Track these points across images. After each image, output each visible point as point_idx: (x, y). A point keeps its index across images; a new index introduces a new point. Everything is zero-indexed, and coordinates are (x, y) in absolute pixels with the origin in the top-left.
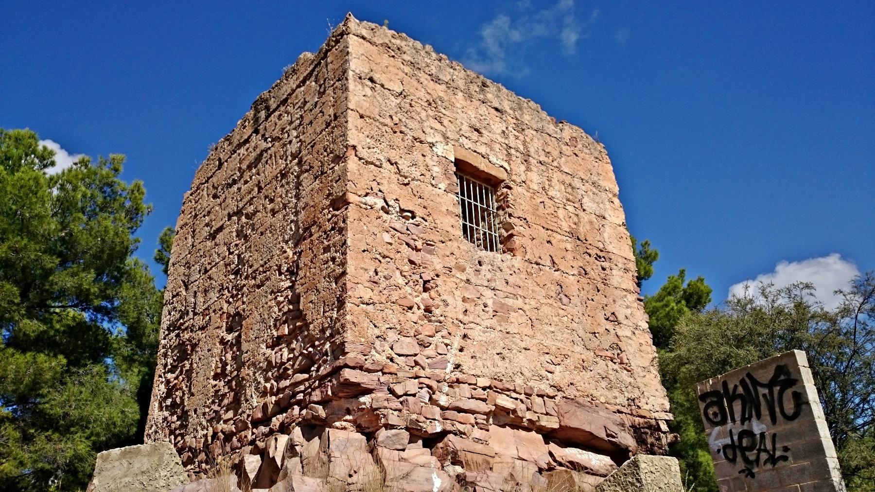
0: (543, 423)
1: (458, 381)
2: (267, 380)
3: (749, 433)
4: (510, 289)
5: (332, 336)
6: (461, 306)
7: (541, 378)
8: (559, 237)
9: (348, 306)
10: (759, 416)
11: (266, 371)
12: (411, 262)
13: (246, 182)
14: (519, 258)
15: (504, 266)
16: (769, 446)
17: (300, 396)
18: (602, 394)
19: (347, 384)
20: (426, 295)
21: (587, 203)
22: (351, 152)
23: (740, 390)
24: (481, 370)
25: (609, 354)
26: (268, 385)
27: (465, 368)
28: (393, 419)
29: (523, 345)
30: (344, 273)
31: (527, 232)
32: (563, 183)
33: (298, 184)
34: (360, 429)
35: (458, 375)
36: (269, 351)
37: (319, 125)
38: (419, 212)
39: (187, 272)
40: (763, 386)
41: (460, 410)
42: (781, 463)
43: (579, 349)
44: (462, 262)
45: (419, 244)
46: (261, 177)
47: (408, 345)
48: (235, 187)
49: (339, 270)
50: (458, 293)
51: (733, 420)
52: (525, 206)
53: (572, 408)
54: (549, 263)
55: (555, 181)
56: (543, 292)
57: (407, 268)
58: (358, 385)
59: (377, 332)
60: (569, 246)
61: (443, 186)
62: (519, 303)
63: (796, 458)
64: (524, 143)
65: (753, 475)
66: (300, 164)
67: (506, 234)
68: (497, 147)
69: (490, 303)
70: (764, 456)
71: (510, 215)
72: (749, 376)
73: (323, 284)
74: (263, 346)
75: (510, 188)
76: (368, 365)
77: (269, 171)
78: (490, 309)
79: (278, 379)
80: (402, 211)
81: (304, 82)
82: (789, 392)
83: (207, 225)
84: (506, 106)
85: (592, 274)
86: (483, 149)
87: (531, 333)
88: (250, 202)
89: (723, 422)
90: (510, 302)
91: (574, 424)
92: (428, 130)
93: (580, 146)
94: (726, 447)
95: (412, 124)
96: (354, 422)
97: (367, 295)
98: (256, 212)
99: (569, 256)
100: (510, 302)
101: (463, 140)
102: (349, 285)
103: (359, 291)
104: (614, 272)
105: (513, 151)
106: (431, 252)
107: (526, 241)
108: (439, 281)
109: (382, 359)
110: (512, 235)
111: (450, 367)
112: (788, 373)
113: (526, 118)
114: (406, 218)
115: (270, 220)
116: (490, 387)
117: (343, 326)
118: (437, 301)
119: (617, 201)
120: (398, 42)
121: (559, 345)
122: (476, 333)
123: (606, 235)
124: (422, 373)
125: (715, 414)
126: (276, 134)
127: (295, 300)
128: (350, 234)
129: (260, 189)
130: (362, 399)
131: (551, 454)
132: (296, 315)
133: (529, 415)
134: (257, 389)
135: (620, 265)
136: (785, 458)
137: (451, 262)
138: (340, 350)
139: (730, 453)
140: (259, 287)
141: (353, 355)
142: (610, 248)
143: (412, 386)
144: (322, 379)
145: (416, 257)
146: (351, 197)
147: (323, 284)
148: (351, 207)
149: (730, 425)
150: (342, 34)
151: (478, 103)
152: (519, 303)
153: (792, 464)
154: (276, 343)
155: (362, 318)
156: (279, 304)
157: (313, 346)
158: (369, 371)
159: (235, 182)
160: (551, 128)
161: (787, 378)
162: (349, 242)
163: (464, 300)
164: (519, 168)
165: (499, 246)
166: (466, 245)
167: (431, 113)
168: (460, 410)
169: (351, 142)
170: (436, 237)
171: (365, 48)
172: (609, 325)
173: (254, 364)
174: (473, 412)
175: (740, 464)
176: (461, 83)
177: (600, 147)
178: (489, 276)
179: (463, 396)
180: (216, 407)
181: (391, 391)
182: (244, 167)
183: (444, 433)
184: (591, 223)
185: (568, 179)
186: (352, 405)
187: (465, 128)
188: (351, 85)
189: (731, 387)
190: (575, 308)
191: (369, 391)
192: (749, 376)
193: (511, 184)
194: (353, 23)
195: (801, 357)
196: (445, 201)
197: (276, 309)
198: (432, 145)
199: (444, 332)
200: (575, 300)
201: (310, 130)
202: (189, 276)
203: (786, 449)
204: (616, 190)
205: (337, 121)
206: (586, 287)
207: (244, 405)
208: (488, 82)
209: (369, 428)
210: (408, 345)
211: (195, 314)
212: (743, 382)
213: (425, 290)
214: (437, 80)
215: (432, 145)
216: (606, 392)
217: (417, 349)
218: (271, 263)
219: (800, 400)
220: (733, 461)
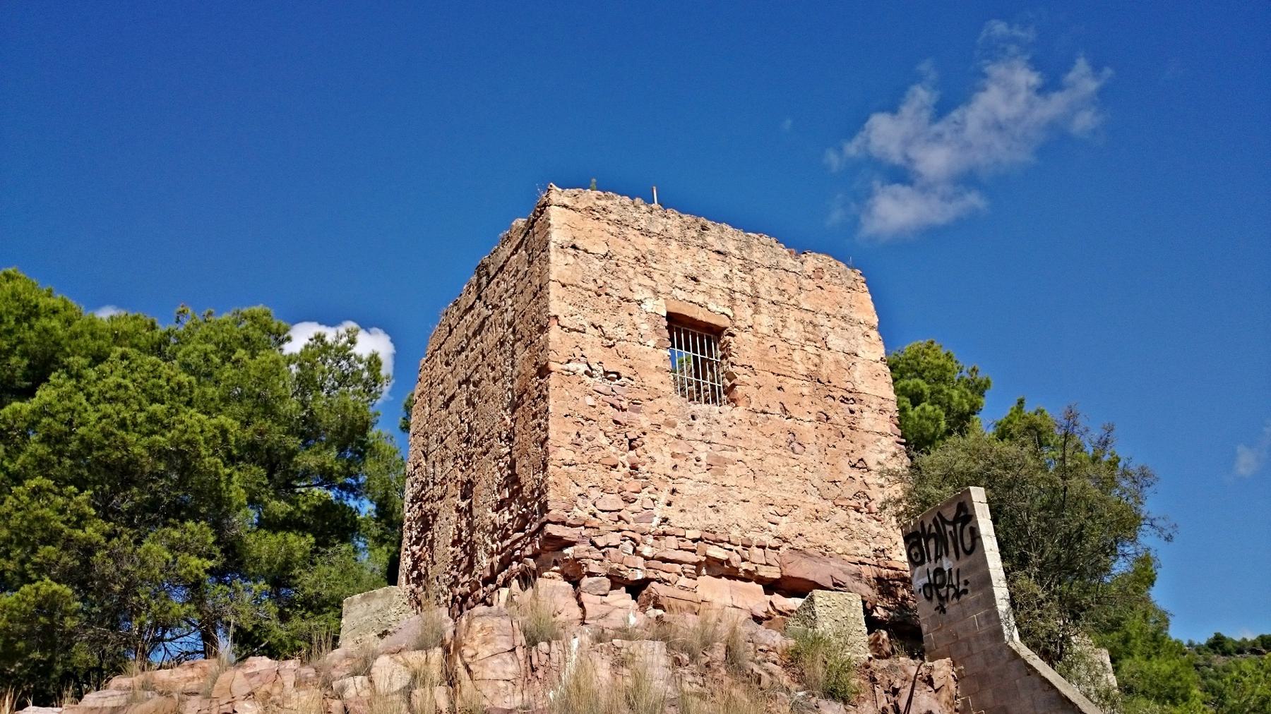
0: (761, 574)
1: (665, 534)
2: (494, 542)
3: (939, 571)
4: (728, 441)
5: (539, 496)
6: (670, 462)
7: (763, 529)
8: (794, 382)
9: (551, 468)
10: (947, 555)
11: (492, 533)
12: (616, 422)
13: (472, 350)
14: (741, 408)
15: (722, 418)
16: (955, 582)
17: (517, 553)
18: (839, 544)
19: (550, 538)
20: (632, 453)
21: (833, 341)
22: (553, 323)
23: (934, 529)
24: (691, 522)
25: (854, 503)
26: (495, 546)
27: (672, 521)
28: (594, 567)
29: (742, 497)
30: (547, 438)
31: (752, 380)
32: (802, 322)
33: (513, 353)
34: (567, 578)
35: (666, 528)
36: (494, 515)
37: (528, 296)
38: (625, 372)
39: (425, 442)
40: (949, 523)
41: (665, 560)
42: (963, 597)
43: (813, 498)
44: (672, 418)
45: (625, 404)
46: (484, 345)
47: (613, 501)
48: (464, 354)
49: (543, 436)
50: (666, 449)
51: (930, 560)
52: (751, 352)
53: (797, 558)
54: (778, 411)
55: (791, 321)
56: (770, 442)
57: (611, 428)
58: (560, 538)
59: (579, 490)
60: (805, 391)
61: (652, 343)
62: (740, 454)
63: (973, 591)
64: (753, 284)
65: (944, 611)
66: (514, 333)
67: (729, 384)
68: (717, 293)
69: (703, 457)
70: (952, 591)
71: (732, 364)
72: (939, 514)
73: (532, 449)
74: (490, 510)
75: (733, 335)
76: (570, 520)
77: (491, 338)
78: (703, 463)
79: (502, 540)
80: (606, 373)
81: (516, 250)
82: (967, 527)
83: (441, 393)
84: (731, 247)
85: (835, 418)
86: (700, 298)
87: (752, 484)
88: (476, 370)
89: (922, 562)
90: (727, 454)
91: (797, 573)
92: (635, 288)
93: (827, 277)
94: (925, 586)
95: (616, 284)
96: (562, 572)
97: (569, 456)
98: (481, 380)
99: (806, 401)
100: (727, 454)
101: (677, 292)
102: (550, 450)
103: (561, 452)
104: (865, 414)
105: (737, 295)
106: (638, 411)
107: (751, 390)
108: (646, 439)
109: (584, 515)
110: (734, 386)
111: (657, 521)
112: (966, 510)
113: (757, 256)
114: (612, 379)
115: (492, 388)
116: (701, 539)
117: (546, 487)
118: (644, 458)
119: (875, 335)
120: (603, 203)
121: (787, 495)
122: (686, 487)
123: (857, 375)
124: (625, 527)
125: (916, 555)
126: (495, 301)
127: (512, 466)
128: (551, 401)
129: (484, 356)
130: (566, 551)
131: (771, 603)
132: (513, 480)
133: (744, 566)
134: (486, 550)
135: (874, 406)
136: (965, 591)
137: (660, 419)
138: (544, 508)
139: (927, 590)
140: (485, 454)
141: (555, 512)
142: (861, 388)
143: (614, 539)
144: (533, 535)
145: (620, 416)
146: (553, 366)
147: (532, 449)
148: (553, 375)
149: (927, 564)
150: (545, 205)
151: (693, 249)
152: (740, 454)
153: (970, 597)
154: (499, 507)
155: (564, 478)
156: (500, 469)
157: (526, 507)
158: (572, 526)
159: (463, 349)
160: (789, 262)
161: (965, 515)
162: (550, 410)
163: (673, 455)
164: (744, 313)
165: (724, 396)
166: (677, 400)
167: (639, 269)
168: (665, 560)
169: (553, 313)
170: (642, 395)
171: (565, 216)
172: (855, 473)
173: (482, 528)
174: (680, 562)
175: (936, 602)
176: (675, 232)
177: (855, 274)
178: (703, 429)
179: (669, 547)
180: (454, 573)
181: (593, 544)
182: (470, 334)
183: (646, 582)
184: (837, 362)
185: (808, 317)
186: (558, 557)
187: (679, 279)
188: (553, 257)
189: (927, 526)
190: (811, 457)
191: (572, 544)
192: (939, 514)
193: (734, 331)
194: (554, 197)
195: (978, 495)
196: (654, 357)
197: (498, 475)
198: (640, 302)
199: (651, 488)
200: (809, 448)
201: (521, 299)
202: (427, 446)
203: (966, 583)
204: (875, 320)
205: (540, 293)
206: (827, 433)
207: (476, 566)
208: (709, 224)
209: (574, 575)
210: (613, 501)
211: (435, 484)
212: (935, 520)
213: (632, 448)
214: (647, 233)
215: (640, 302)
216: (846, 543)
217: (622, 505)
218: (494, 431)
219: (975, 535)
220: (929, 599)
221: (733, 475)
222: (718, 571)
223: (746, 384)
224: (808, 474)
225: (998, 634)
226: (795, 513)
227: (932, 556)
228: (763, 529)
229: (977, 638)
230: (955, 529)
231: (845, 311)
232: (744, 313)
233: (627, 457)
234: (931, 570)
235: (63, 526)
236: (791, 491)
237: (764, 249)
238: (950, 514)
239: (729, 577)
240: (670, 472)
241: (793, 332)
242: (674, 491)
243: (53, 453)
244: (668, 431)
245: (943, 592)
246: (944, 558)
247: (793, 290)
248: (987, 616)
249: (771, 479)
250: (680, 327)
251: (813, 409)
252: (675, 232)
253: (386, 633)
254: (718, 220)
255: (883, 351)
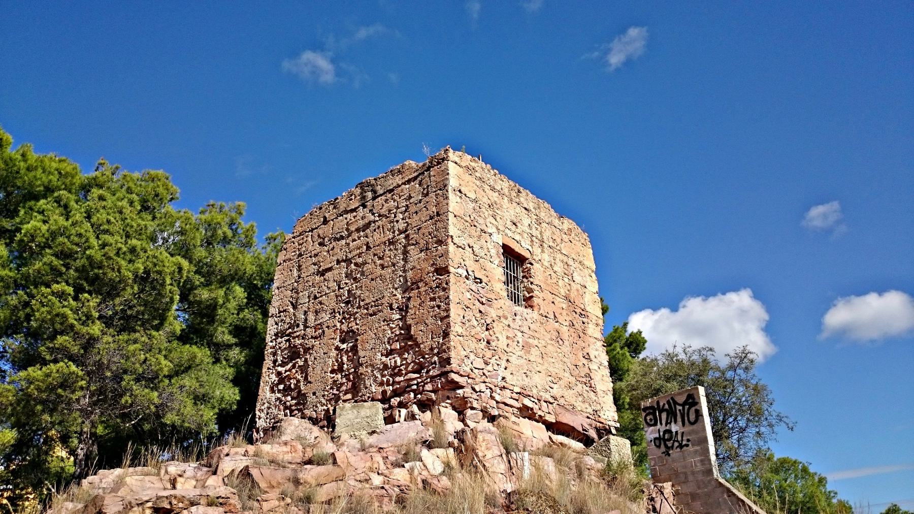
0: (547, 418)
1: (504, 387)
2: (383, 376)
3: (670, 431)
4: (531, 333)
5: (438, 353)
6: (506, 342)
7: (547, 391)
8: (559, 299)
9: (452, 337)
10: (676, 422)
11: (383, 370)
12: (480, 312)
13: (354, 240)
14: (536, 312)
15: (528, 317)
16: (680, 439)
17: (415, 387)
18: (579, 405)
19: (453, 381)
20: (487, 333)
21: (577, 277)
22: (450, 240)
23: (667, 407)
24: (516, 381)
25: (584, 380)
26: (385, 379)
27: (507, 380)
28: (475, 405)
29: (538, 369)
30: (448, 316)
31: (541, 295)
32: (562, 261)
33: (405, 253)
34: (454, 408)
35: (504, 384)
36: (384, 359)
37: (424, 215)
38: (485, 280)
39: (295, 295)
40: (679, 405)
41: (506, 404)
42: (685, 448)
43: (567, 375)
44: (506, 314)
45: (484, 300)
46: (370, 240)
47: (479, 363)
48: (343, 242)
49: (444, 314)
50: (504, 333)
51: (661, 424)
52: (540, 277)
53: (563, 411)
54: (552, 317)
55: (558, 260)
56: (548, 336)
57: (478, 315)
58: (457, 383)
59: (465, 353)
60: (564, 306)
61: (496, 262)
62: (536, 342)
63: (693, 445)
64: (541, 233)
65: (669, 455)
66: (407, 237)
67: (528, 295)
68: (525, 235)
69: (520, 341)
70: (676, 444)
71: (532, 283)
72: (672, 398)
73: (430, 321)
74: (379, 354)
75: (532, 264)
76: (461, 373)
77: (377, 238)
78: (520, 345)
79: (393, 375)
80: (476, 278)
81: (409, 182)
82: (693, 409)
83: (314, 264)
84: (531, 206)
85: (577, 326)
86: (518, 237)
87: (541, 362)
88: (359, 255)
89: (655, 424)
90: (531, 341)
91: (564, 421)
92: (489, 225)
93: (573, 235)
94: (655, 439)
95: (481, 221)
96: (451, 404)
97: (460, 330)
98: (365, 263)
99: (564, 313)
100: (531, 341)
101: (507, 231)
102: (452, 324)
103: (456, 328)
104: (590, 325)
105: (534, 239)
106: (490, 306)
107: (540, 301)
108: (494, 325)
109: (468, 369)
110: (532, 297)
111: (500, 378)
112: (694, 399)
113: (542, 215)
114: (477, 283)
115: (379, 271)
116: (520, 393)
117: (448, 348)
118: (494, 338)
119: (593, 275)
120: (473, 164)
121: (557, 371)
122: (513, 359)
123: (586, 300)
124: (487, 380)
125: (651, 420)
126: (383, 212)
127: (408, 328)
128: (451, 293)
129: (368, 248)
130: (458, 391)
131: (550, 438)
132: (407, 337)
133: (540, 413)
134: (375, 381)
135: (594, 321)
136: (687, 445)
137: (500, 313)
138: (448, 361)
139: (657, 442)
140: (371, 315)
141: (454, 365)
142: (588, 309)
143: (482, 387)
144: (432, 378)
145: (482, 308)
146: (451, 269)
147: (430, 321)
148: (452, 275)
149: (659, 426)
150: (443, 159)
151: (515, 204)
152: (536, 342)
153: (691, 448)
154: (389, 353)
155: (458, 344)
156: (391, 328)
157: (424, 358)
158: (461, 376)
159: (342, 238)
160: (556, 222)
161: (692, 401)
162: (451, 297)
163: (508, 338)
164: (537, 250)
165: (524, 303)
166: (509, 303)
167: (491, 213)
168: (506, 404)
169: (451, 234)
170: (493, 297)
171: (459, 169)
172: (585, 361)
173: (371, 365)
174: (512, 406)
175: (663, 449)
176: (506, 191)
177: (585, 236)
178: (520, 323)
179: (506, 396)
180: (335, 392)
181: (474, 389)
182: (352, 228)
183: (500, 416)
184: (578, 290)
185: (565, 259)
186: (451, 394)
187: (509, 223)
188: (451, 195)
189: (661, 404)
190: (566, 348)
191: (462, 387)
192: (672, 398)
193: (533, 262)
194: (453, 155)
195: (702, 390)
196: (496, 271)
197: (389, 332)
198: (491, 235)
199: (497, 357)
200: (566, 343)
201: (416, 217)
202: (297, 299)
203: (688, 440)
204: (594, 267)
205: (439, 216)
206: (573, 334)
207: (364, 391)
208: (521, 189)
209: (461, 409)
210: (479, 363)
211: (306, 327)
212: (668, 402)
213: (487, 329)
214: (493, 189)
215: (491, 235)
216: (581, 404)
217: (483, 366)
218: (383, 301)
219: (698, 414)
220: (659, 447)
221: (535, 354)
222: (525, 414)
223: (539, 298)
224: (565, 360)
225: (710, 472)
226: (561, 382)
227: (664, 422)
228: (547, 391)
229: (693, 473)
230: (684, 409)
231: (581, 259)
232: (537, 250)
233: (485, 335)
234: (662, 430)
235: (75, 322)
236: (557, 369)
237: (547, 212)
238: (681, 399)
239: (529, 419)
240: (506, 348)
241: (559, 268)
242: (508, 360)
243: (63, 265)
244: (504, 321)
245: (669, 444)
246: (673, 424)
247: (559, 240)
248: (702, 461)
249: (550, 360)
250: (508, 252)
251: (568, 318)
252: (506, 191)
253: (374, 432)
254: (525, 188)
255: (597, 287)
